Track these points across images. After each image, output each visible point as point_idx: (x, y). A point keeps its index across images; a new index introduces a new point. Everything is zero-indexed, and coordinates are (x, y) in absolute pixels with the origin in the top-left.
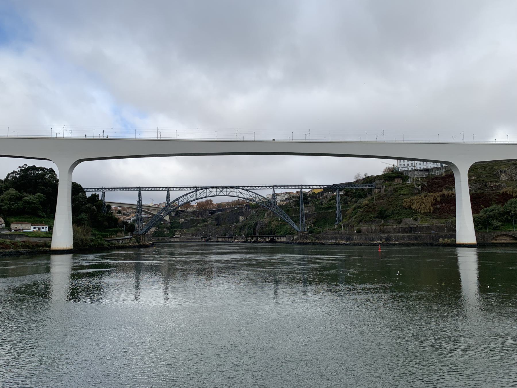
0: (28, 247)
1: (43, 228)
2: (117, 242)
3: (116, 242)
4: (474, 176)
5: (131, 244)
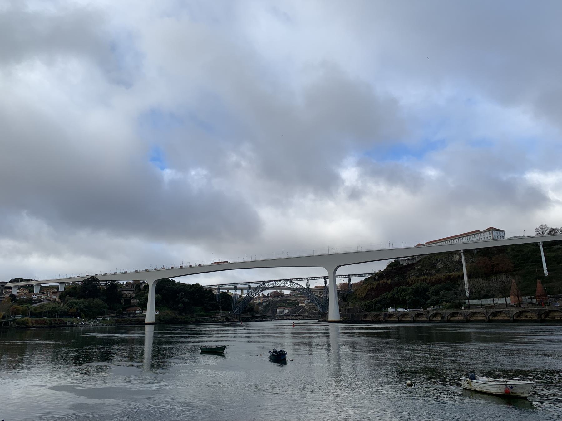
0: (137, 322)
1: (157, 313)
3: (210, 319)
4: (419, 265)
5: (220, 321)
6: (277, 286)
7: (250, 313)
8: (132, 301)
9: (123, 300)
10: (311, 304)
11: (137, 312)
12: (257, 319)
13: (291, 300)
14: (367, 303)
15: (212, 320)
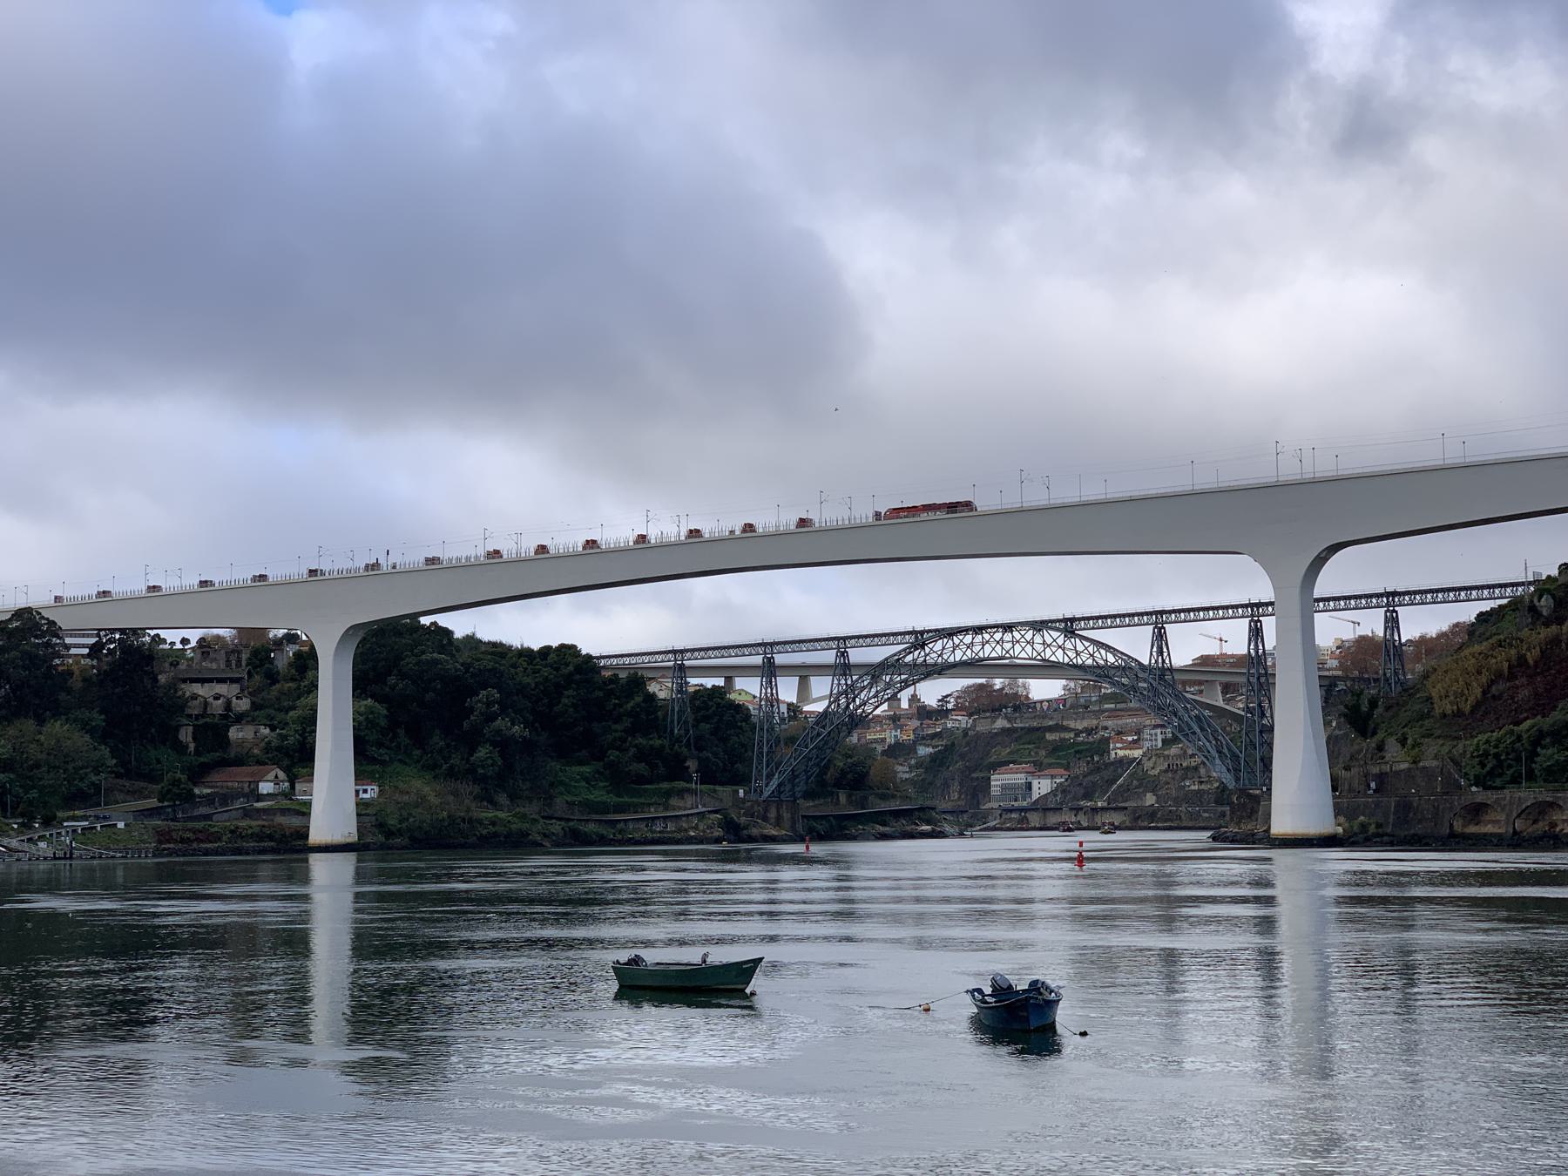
0: (271, 838)
1: (365, 791)
2: (647, 826)
3: (642, 825)
6: (994, 655)
7: (849, 796)
8: (234, 733)
9: (190, 729)
10: (1174, 750)
11: (266, 788)
12: (884, 824)
13: (1067, 729)
14: (1488, 742)
15: (655, 832)
